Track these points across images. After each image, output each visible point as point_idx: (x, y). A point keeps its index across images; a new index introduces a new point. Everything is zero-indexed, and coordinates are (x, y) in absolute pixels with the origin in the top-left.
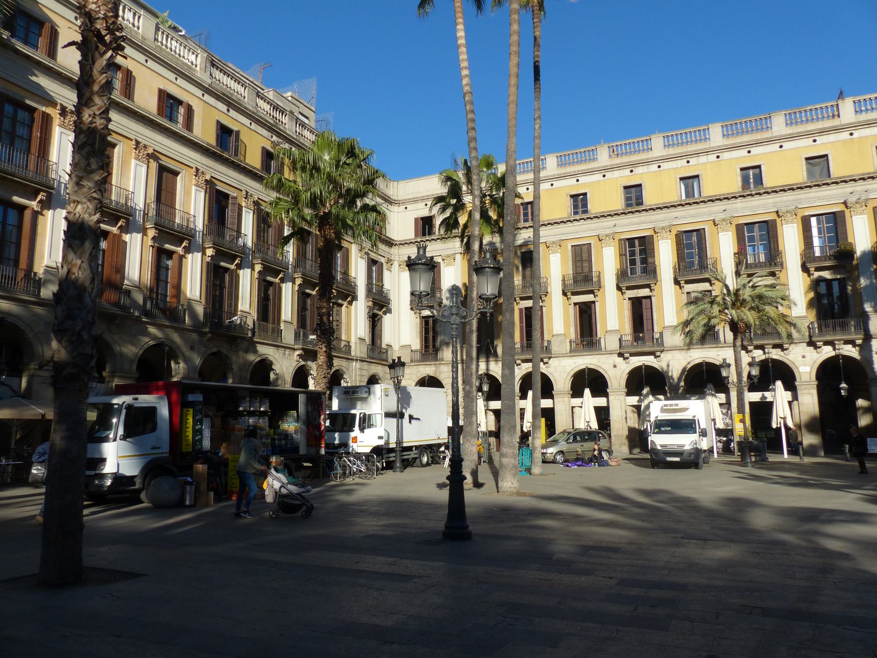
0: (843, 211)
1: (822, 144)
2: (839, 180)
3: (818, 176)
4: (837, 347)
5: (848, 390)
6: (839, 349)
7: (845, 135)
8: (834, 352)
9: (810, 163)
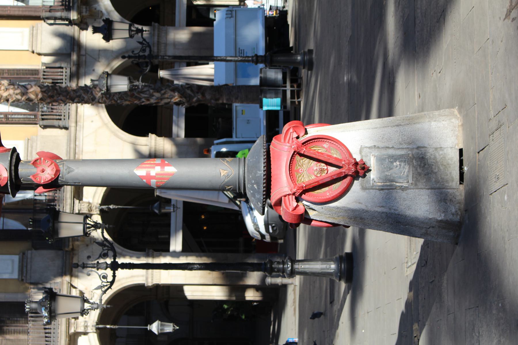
4: (81, 329)
5: (165, 318)
6: (86, 327)
8: (90, 335)
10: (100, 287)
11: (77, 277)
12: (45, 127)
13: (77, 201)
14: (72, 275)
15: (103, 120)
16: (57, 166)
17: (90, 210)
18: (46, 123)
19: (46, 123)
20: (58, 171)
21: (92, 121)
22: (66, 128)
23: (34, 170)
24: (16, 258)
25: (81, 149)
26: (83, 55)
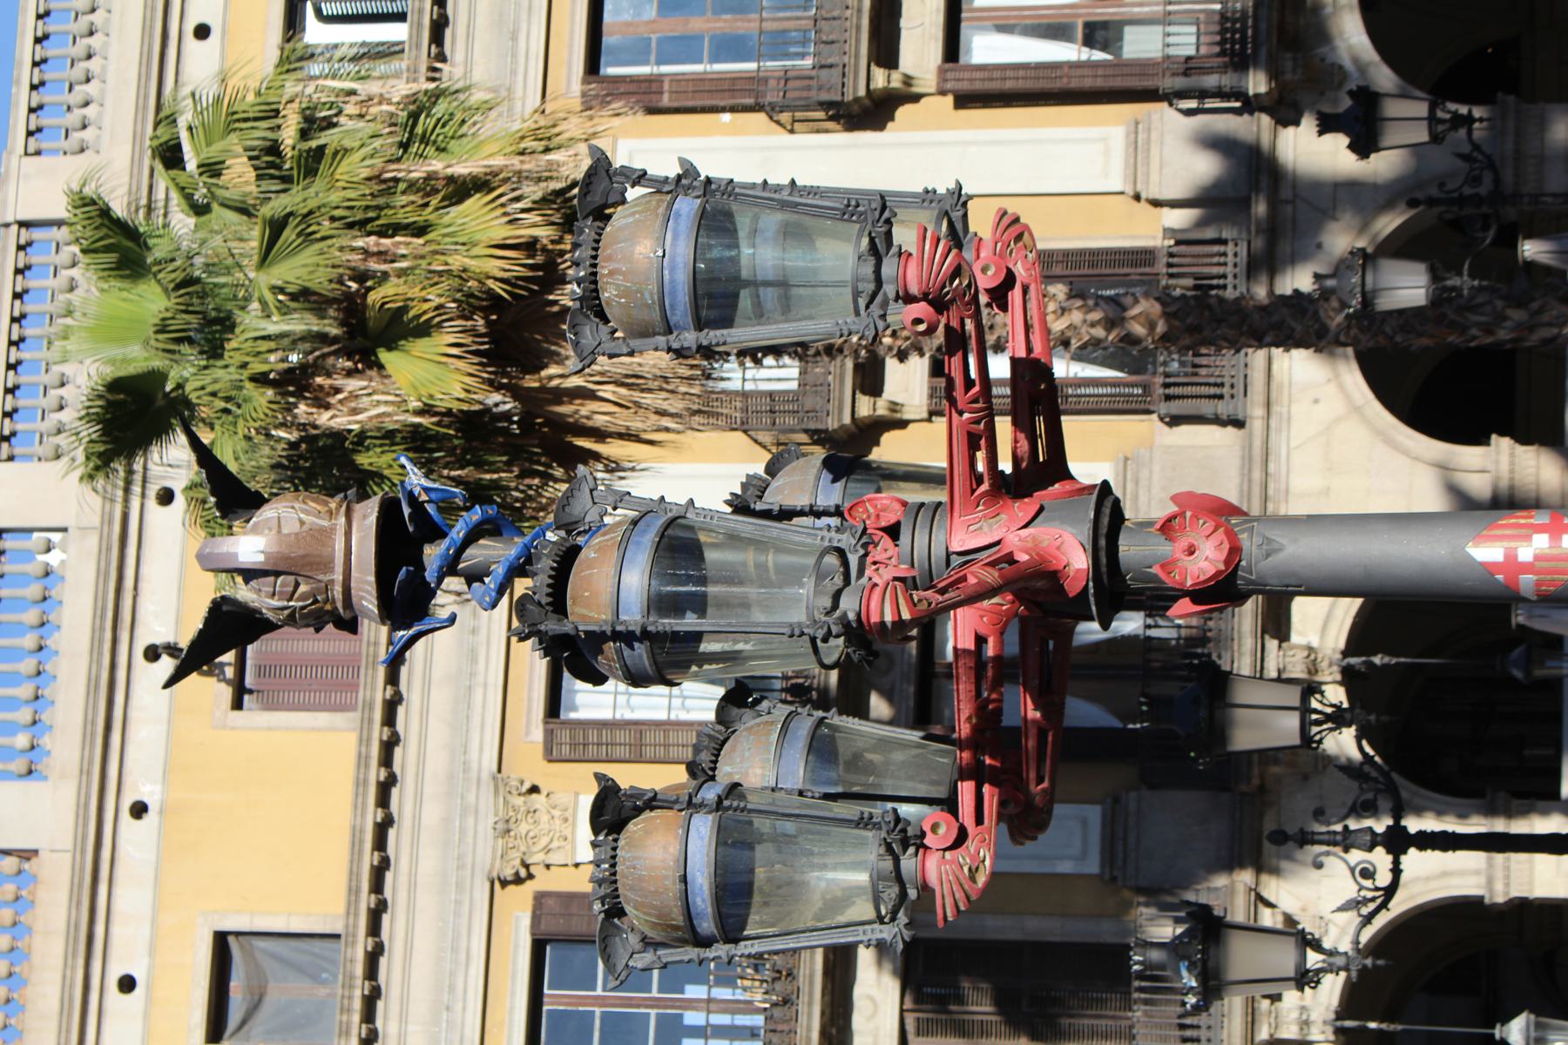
0: (540, 898)
1: (152, 951)
2: (366, 900)
3: (323, 991)
7: (135, 839)
9: (243, 1023)
10: (1354, 905)
11: (1276, 871)
12: (1175, 421)
13: (1272, 644)
14: (1260, 867)
15: (1347, 397)
16: (1231, 535)
17: (1313, 668)
18: (1176, 407)
19: (1176, 407)
20: (1235, 550)
21: (1316, 401)
22: (1239, 424)
23: (1164, 549)
24: (1094, 813)
25: (1283, 486)
26: (1287, 202)
